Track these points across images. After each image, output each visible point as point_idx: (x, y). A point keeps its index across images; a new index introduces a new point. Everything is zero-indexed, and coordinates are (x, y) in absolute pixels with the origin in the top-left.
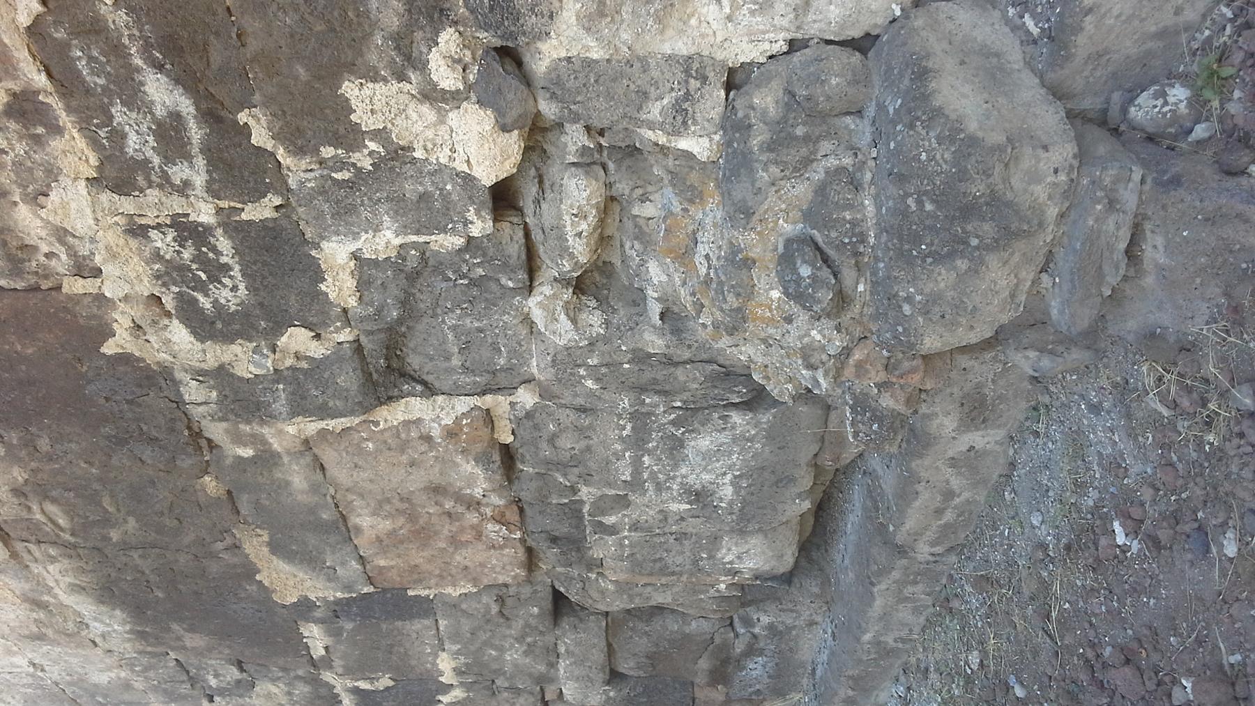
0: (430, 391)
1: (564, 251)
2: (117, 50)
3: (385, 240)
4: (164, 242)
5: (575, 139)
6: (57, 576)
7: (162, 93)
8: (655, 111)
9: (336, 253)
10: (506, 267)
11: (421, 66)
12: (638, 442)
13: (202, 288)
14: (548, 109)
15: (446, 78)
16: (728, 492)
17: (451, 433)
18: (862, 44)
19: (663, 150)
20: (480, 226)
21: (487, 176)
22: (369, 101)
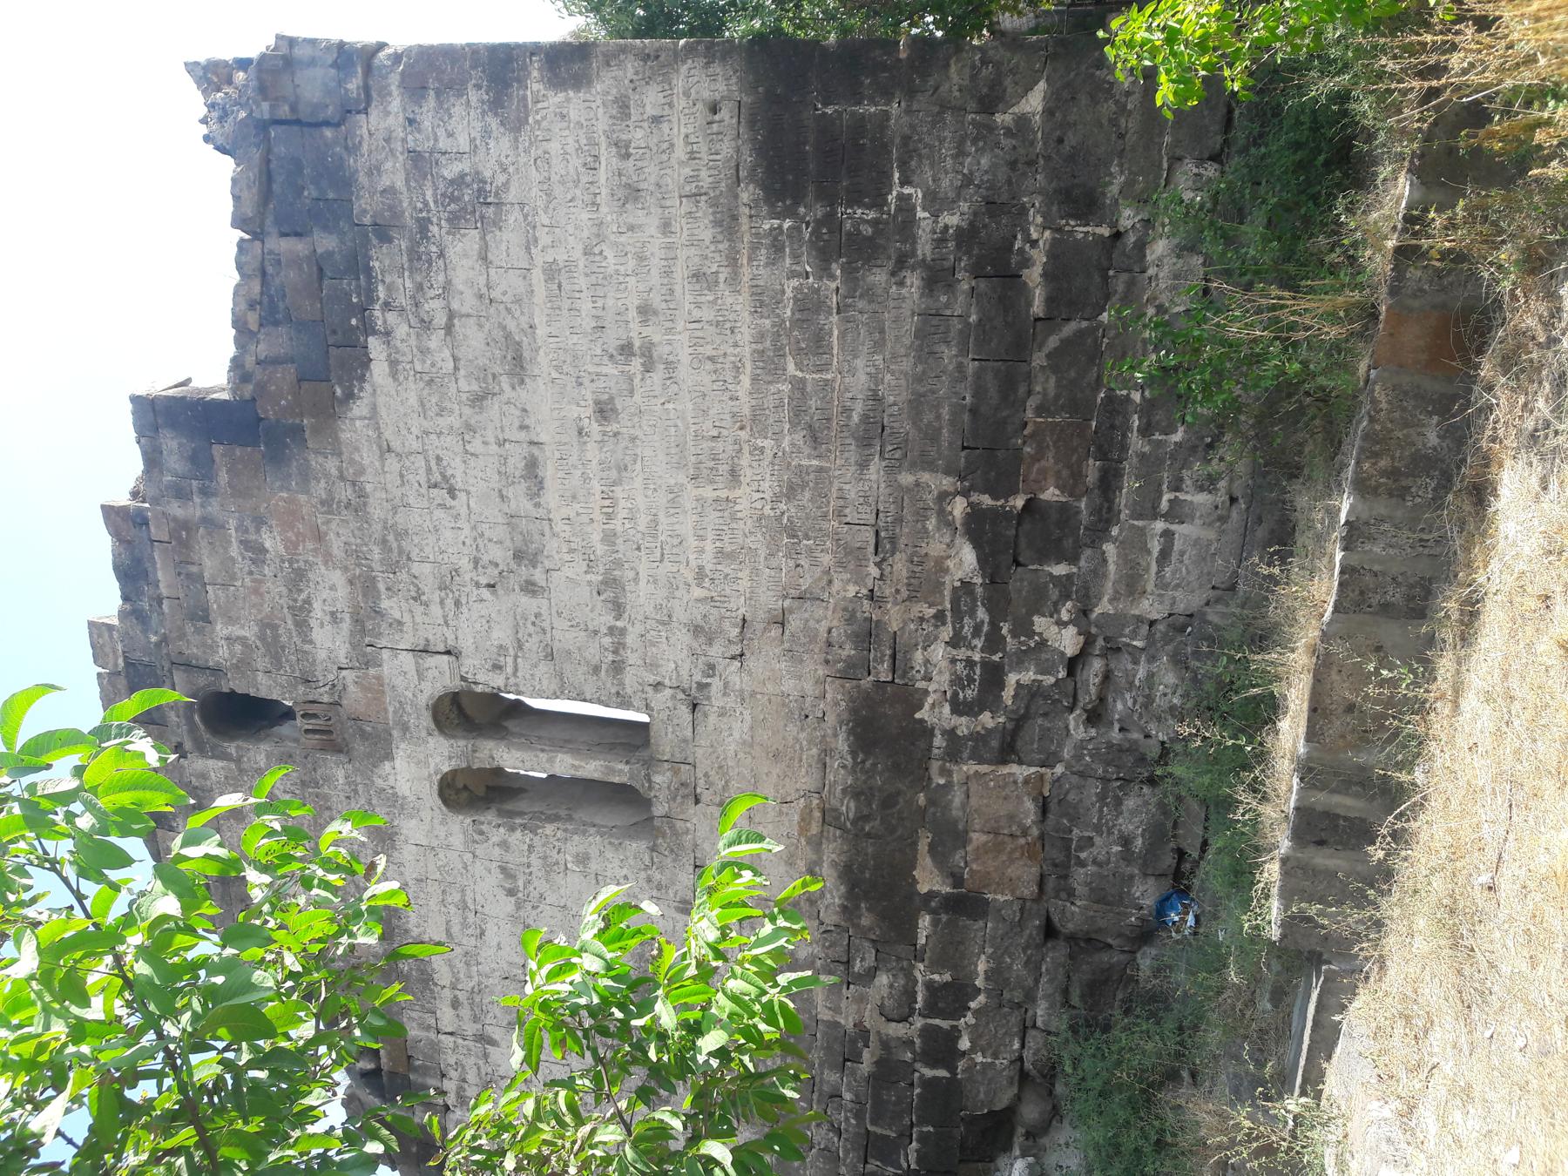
0: (1020, 763)
1: (1088, 692)
2: (974, 600)
3: (1028, 676)
4: (959, 666)
5: (1100, 642)
6: (832, 852)
7: (982, 614)
8: (1127, 631)
9: (1012, 679)
10: (1066, 695)
11: (1058, 612)
12: (1102, 797)
13: (963, 689)
14: (1094, 630)
15: (1065, 616)
16: (1139, 842)
17: (1027, 781)
18: (1191, 616)
19: (1129, 645)
20: (1062, 674)
21: (1070, 651)
22: (1040, 623)
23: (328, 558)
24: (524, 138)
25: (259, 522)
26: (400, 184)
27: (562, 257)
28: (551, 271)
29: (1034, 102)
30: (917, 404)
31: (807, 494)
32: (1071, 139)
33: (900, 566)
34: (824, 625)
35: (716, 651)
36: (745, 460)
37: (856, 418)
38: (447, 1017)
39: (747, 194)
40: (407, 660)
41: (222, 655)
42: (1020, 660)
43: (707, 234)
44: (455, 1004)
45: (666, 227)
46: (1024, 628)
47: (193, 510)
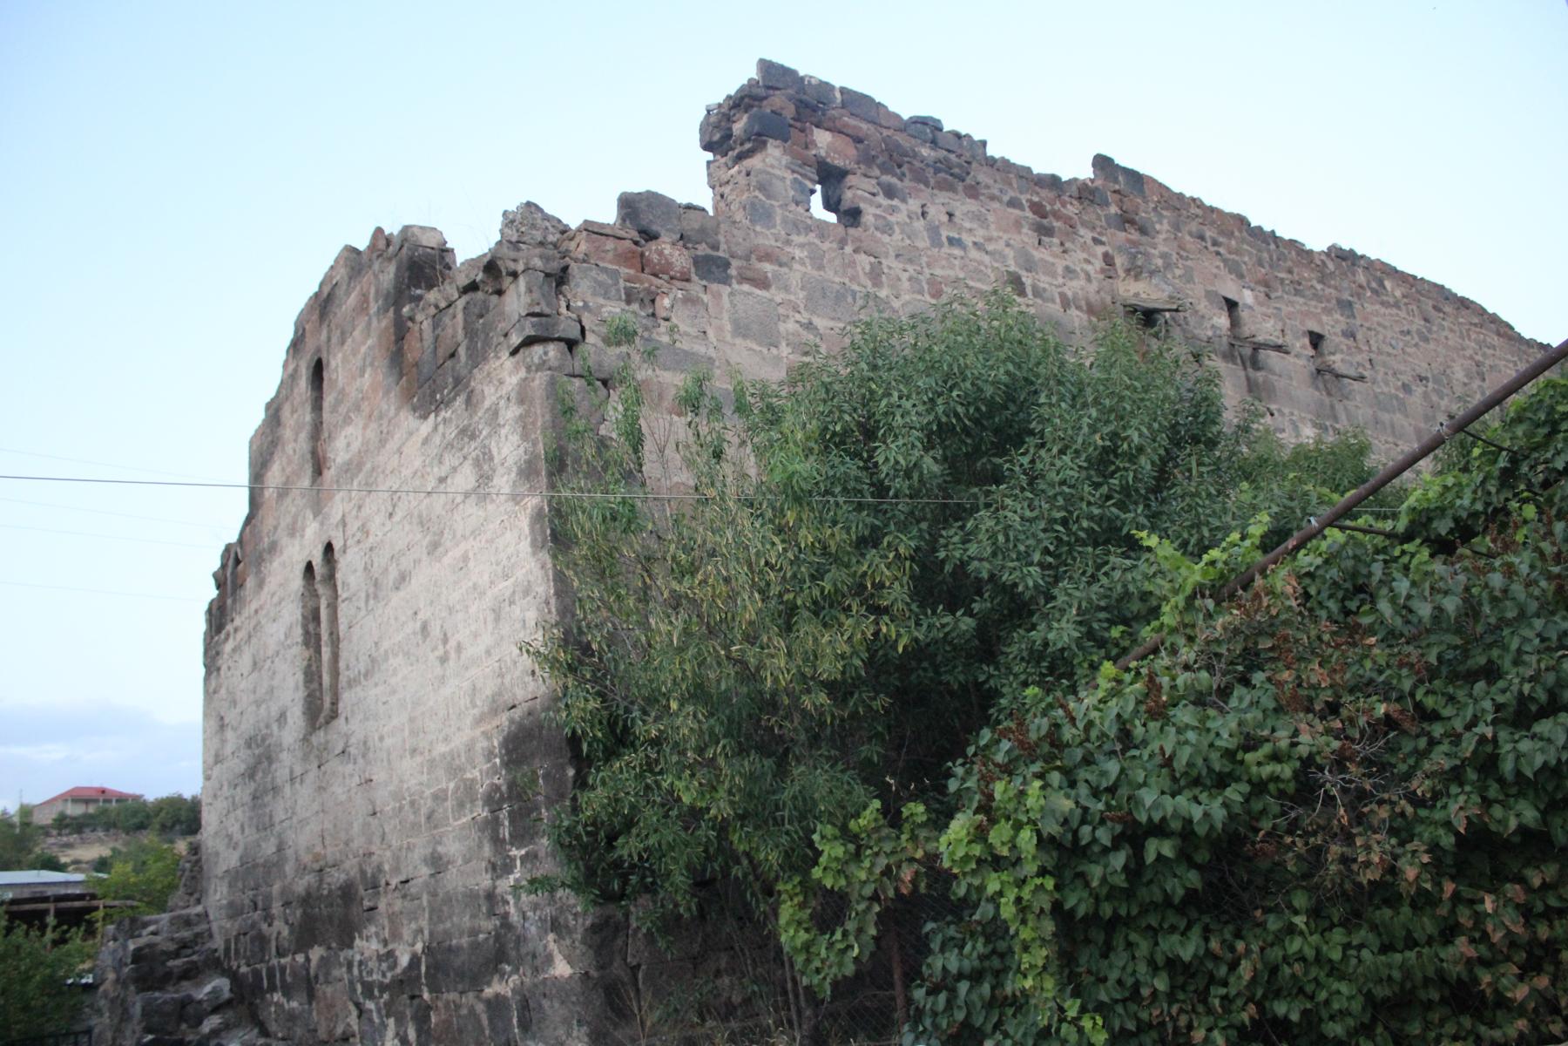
0: (359, 1017)
7: (389, 975)
23: (365, 428)
24: (510, 506)
25: (372, 364)
26: (487, 404)
27: (471, 564)
28: (465, 559)
29: (562, 968)
30: (448, 900)
31: (412, 817)
32: (546, 1003)
33: (398, 905)
34: (373, 848)
35: (360, 761)
36: (419, 759)
37: (440, 849)
38: (254, 606)
39: (504, 719)
40: (339, 516)
41: (333, 364)
42: (379, 1010)
43: (488, 692)
44: (256, 612)
45: (488, 653)
46: (389, 1010)
47: (373, 308)
